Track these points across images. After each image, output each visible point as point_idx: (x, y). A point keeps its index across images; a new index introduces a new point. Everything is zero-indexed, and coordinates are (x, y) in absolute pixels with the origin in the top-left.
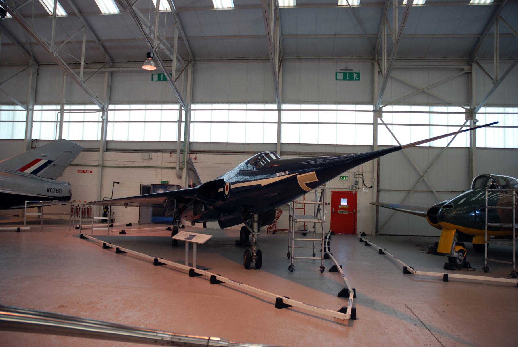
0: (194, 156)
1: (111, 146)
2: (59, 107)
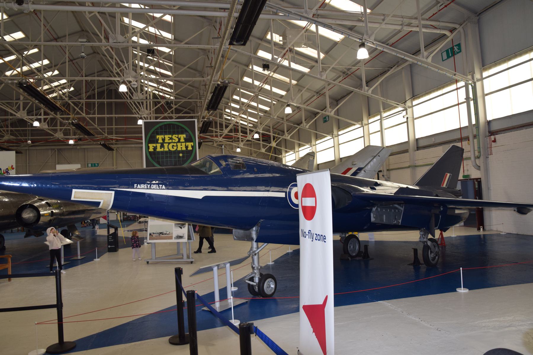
0: (493, 138)
1: (421, 144)
2: (378, 117)
